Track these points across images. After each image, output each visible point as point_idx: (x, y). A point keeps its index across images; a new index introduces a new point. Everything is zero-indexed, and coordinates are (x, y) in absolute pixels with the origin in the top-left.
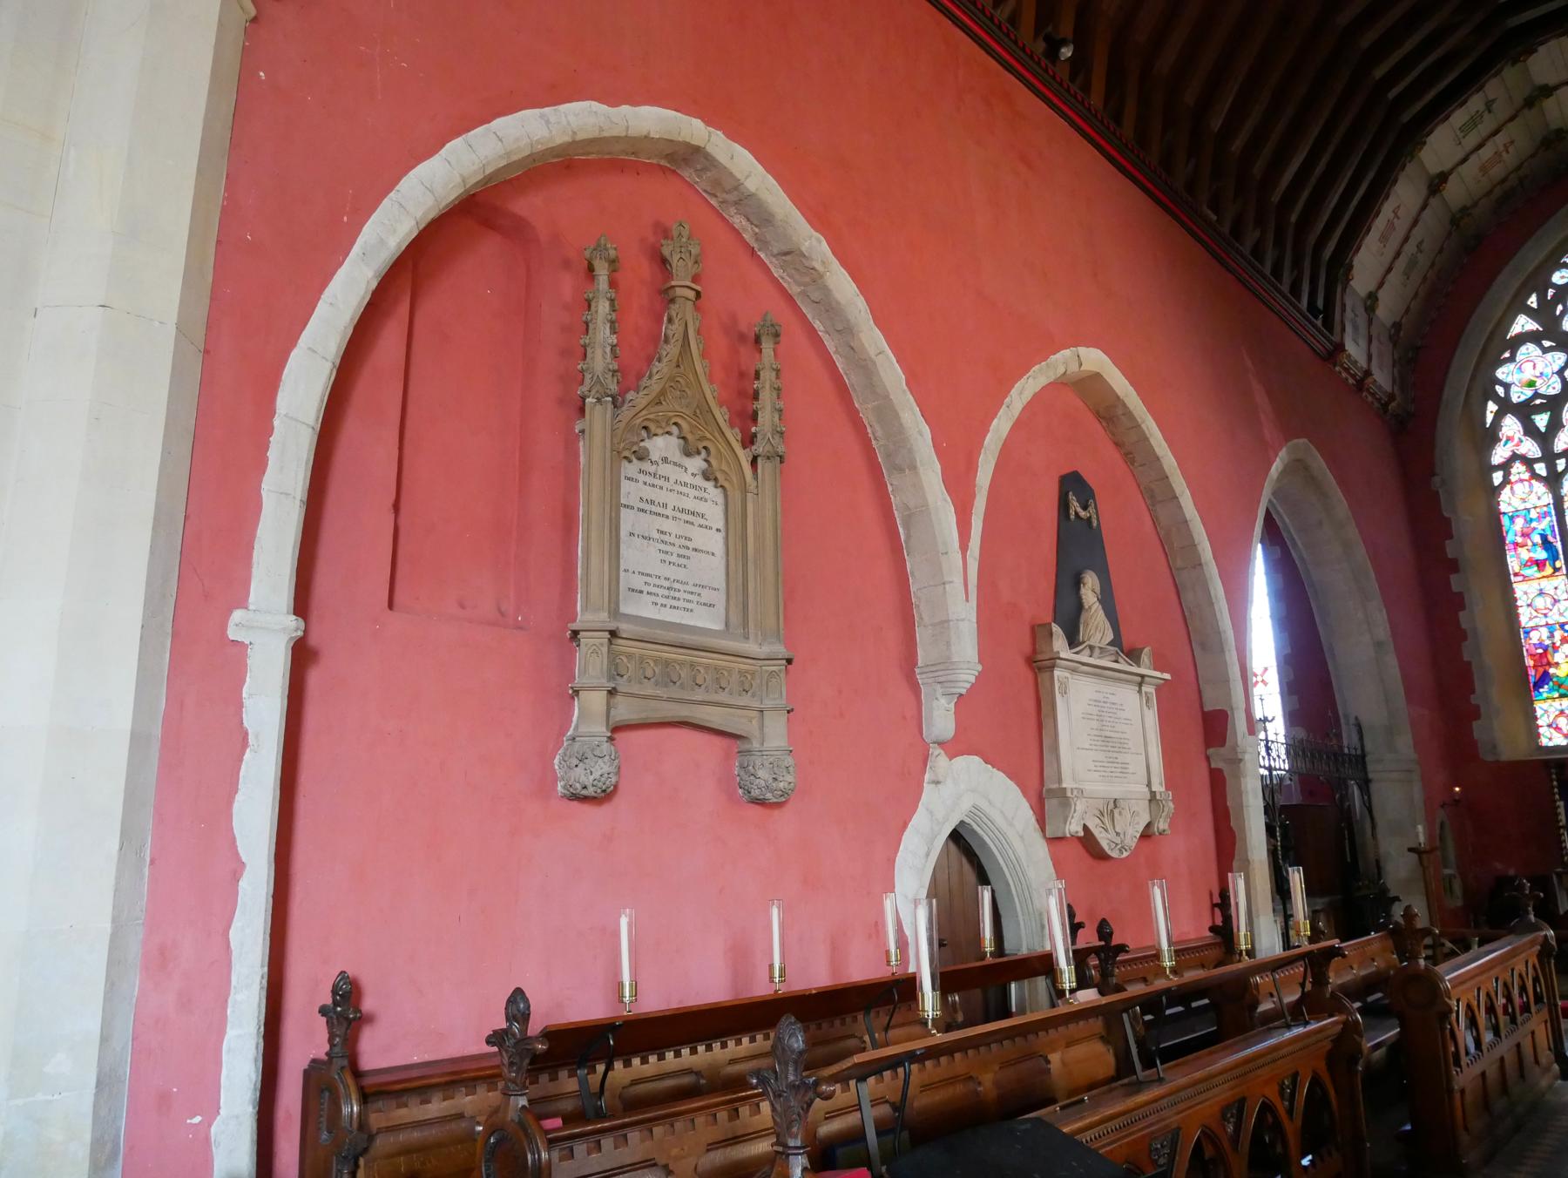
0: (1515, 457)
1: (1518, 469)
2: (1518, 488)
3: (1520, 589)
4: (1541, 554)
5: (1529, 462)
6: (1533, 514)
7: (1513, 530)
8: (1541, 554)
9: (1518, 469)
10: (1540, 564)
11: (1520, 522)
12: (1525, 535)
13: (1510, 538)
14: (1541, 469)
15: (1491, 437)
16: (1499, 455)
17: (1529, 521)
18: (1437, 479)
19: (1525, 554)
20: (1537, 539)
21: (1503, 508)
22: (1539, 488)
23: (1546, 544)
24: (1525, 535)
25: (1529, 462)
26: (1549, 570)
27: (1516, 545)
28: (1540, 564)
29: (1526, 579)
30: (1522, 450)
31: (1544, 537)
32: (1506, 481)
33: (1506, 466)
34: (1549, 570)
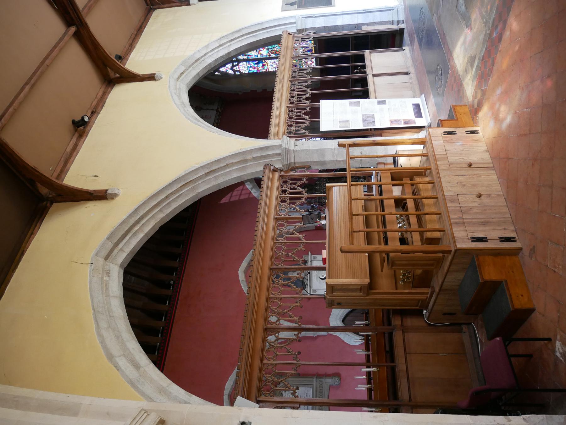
0: (232, 69)
1: (235, 68)
2: (241, 69)
3: (270, 70)
4: (261, 65)
5: (233, 66)
6: (249, 66)
7: (253, 70)
8: (261, 65)
9: (235, 68)
10: (263, 65)
11: (251, 69)
12: (255, 68)
13: (256, 71)
14: (235, 64)
15: (226, 74)
16: (231, 72)
17: (251, 67)
18: (240, 93)
19: (260, 68)
20: (256, 65)
21: (247, 72)
22: (241, 64)
23: (258, 64)
24: (255, 68)
25: (233, 66)
26: (265, 63)
27: (258, 70)
28: (263, 65)
29: (268, 68)
30: (230, 67)
31: (255, 64)
32: (239, 71)
33: (235, 71)
34: (265, 63)
